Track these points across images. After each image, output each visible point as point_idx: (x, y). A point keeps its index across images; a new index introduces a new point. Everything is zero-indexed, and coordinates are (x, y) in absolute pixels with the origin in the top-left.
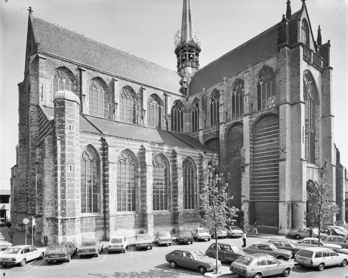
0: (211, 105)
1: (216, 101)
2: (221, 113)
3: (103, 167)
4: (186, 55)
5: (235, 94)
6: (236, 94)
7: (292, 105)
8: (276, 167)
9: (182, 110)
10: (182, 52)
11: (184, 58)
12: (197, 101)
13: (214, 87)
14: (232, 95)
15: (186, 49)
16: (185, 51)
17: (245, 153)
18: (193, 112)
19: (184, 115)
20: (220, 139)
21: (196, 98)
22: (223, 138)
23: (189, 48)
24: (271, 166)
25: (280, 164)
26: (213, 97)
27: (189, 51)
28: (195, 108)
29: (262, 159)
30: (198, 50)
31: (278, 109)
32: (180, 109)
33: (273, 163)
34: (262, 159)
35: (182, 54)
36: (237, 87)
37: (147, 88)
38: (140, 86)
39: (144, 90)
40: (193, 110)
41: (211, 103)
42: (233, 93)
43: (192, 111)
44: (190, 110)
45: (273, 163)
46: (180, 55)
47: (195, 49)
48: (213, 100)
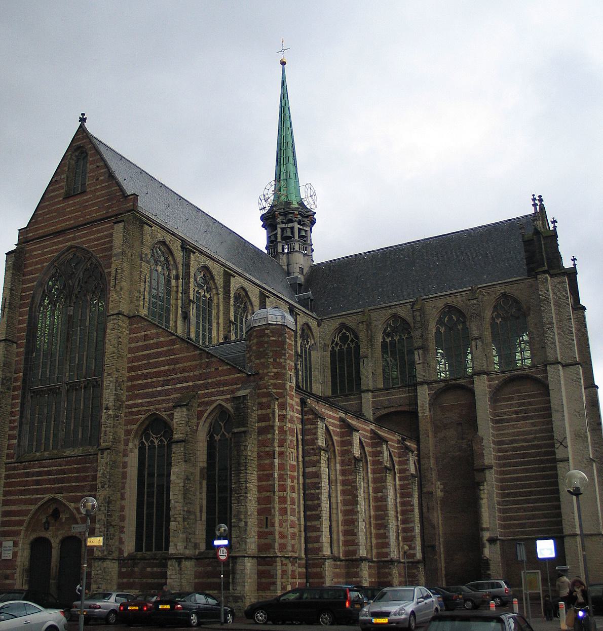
0: (384, 345)
1: (396, 339)
2: (419, 364)
3: (303, 458)
4: (292, 228)
5: (442, 330)
6: (444, 332)
7: (563, 366)
8: (544, 473)
9: (309, 345)
10: (283, 223)
11: (289, 234)
12: (344, 331)
13: (393, 311)
14: (434, 330)
15: (294, 219)
16: (291, 221)
17: (482, 444)
18: (333, 354)
19: (315, 355)
20: (420, 415)
21: (343, 326)
22: (427, 413)
23: (299, 216)
24: (534, 470)
25: (558, 466)
26: (387, 327)
27: (299, 223)
28: (337, 344)
29: (513, 457)
30: (313, 222)
31: (546, 371)
32: (308, 342)
33: (537, 466)
34: (513, 457)
35: (284, 226)
36: (446, 319)
37: (272, 298)
38: (258, 290)
39: (267, 299)
40: (333, 348)
41: (384, 339)
42: (438, 329)
43: (330, 349)
44: (325, 345)
45: (537, 466)
46: (280, 226)
47: (308, 218)
48: (388, 335)
